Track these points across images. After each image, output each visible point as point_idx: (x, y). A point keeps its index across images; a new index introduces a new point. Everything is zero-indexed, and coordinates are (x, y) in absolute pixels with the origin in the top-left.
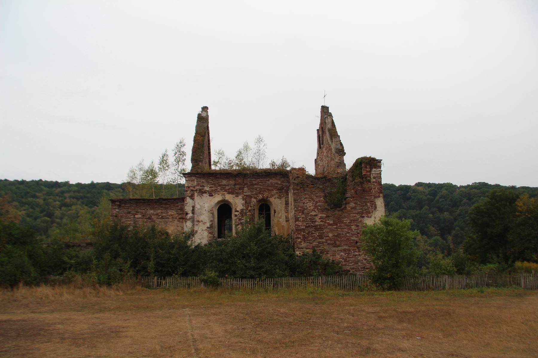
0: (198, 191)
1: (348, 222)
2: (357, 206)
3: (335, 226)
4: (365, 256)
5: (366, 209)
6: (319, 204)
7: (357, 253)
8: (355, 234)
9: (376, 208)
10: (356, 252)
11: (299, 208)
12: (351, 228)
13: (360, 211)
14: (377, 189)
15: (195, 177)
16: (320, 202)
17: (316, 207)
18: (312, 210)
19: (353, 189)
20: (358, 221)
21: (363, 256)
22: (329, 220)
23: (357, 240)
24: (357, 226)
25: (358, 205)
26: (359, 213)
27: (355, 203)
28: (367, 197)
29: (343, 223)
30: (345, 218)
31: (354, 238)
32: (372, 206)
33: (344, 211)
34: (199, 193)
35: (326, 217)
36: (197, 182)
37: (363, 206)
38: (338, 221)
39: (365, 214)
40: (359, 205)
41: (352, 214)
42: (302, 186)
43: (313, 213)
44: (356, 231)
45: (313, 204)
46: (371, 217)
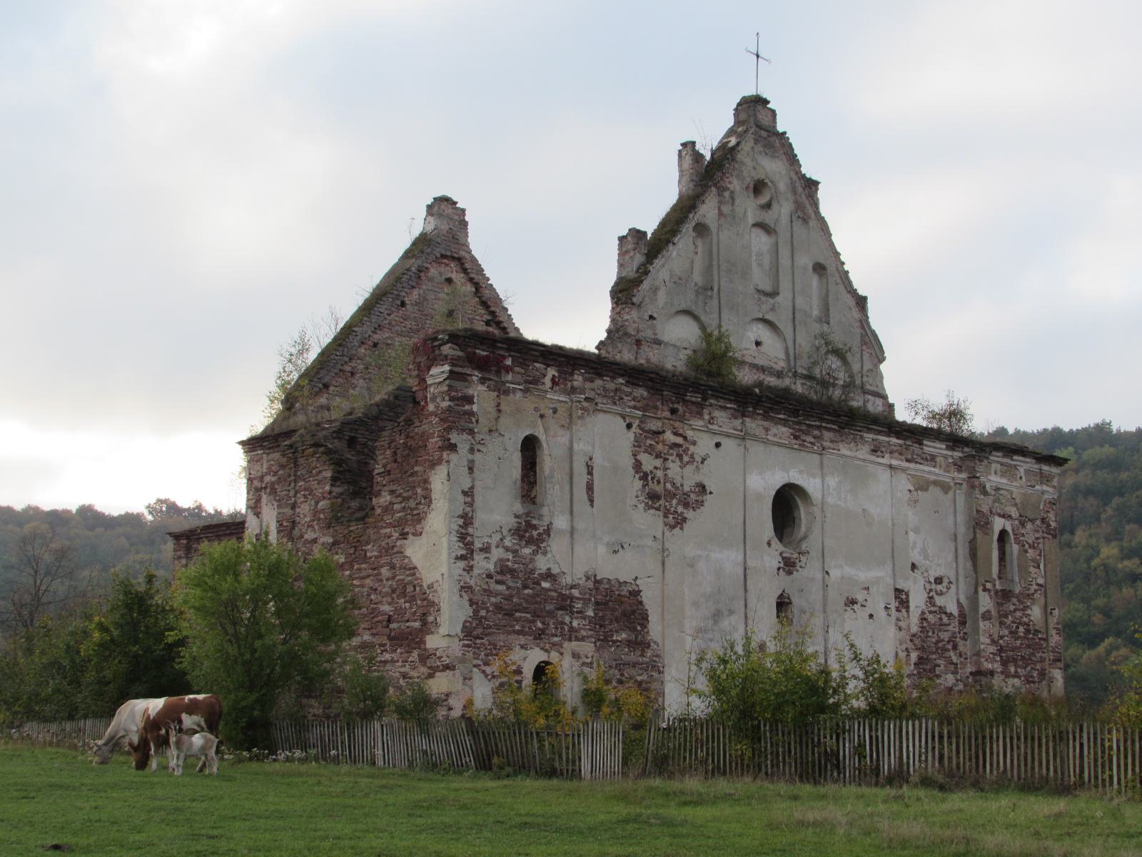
0: (268, 490)
1: (376, 557)
2: (394, 500)
3: (347, 573)
4: (405, 666)
5: (412, 510)
6: (321, 504)
7: (387, 656)
8: (387, 594)
9: (431, 501)
10: (386, 651)
11: (285, 524)
12: (379, 574)
13: (400, 517)
14: (438, 437)
15: (262, 447)
16: (324, 498)
17: (315, 513)
18: (308, 526)
19: (389, 448)
20: (395, 550)
21: (400, 664)
22: (337, 553)
23: (391, 613)
24: (393, 567)
25: (396, 497)
26: (398, 522)
27: (392, 492)
28: (416, 469)
29: (365, 559)
30: (368, 543)
31: (386, 608)
32: (425, 498)
33: (367, 520)
34: (270, 494)
35: (334, 544)
36: (268, 461)
37: (408, 499)
38: (358, 556)
39: (410, 525)
40: (400, 495)
41: (385, 527)
42: (290, 455)
43: (309, 535)
44: (390, 583)
45: (310, 505)
46: (421, 533)
